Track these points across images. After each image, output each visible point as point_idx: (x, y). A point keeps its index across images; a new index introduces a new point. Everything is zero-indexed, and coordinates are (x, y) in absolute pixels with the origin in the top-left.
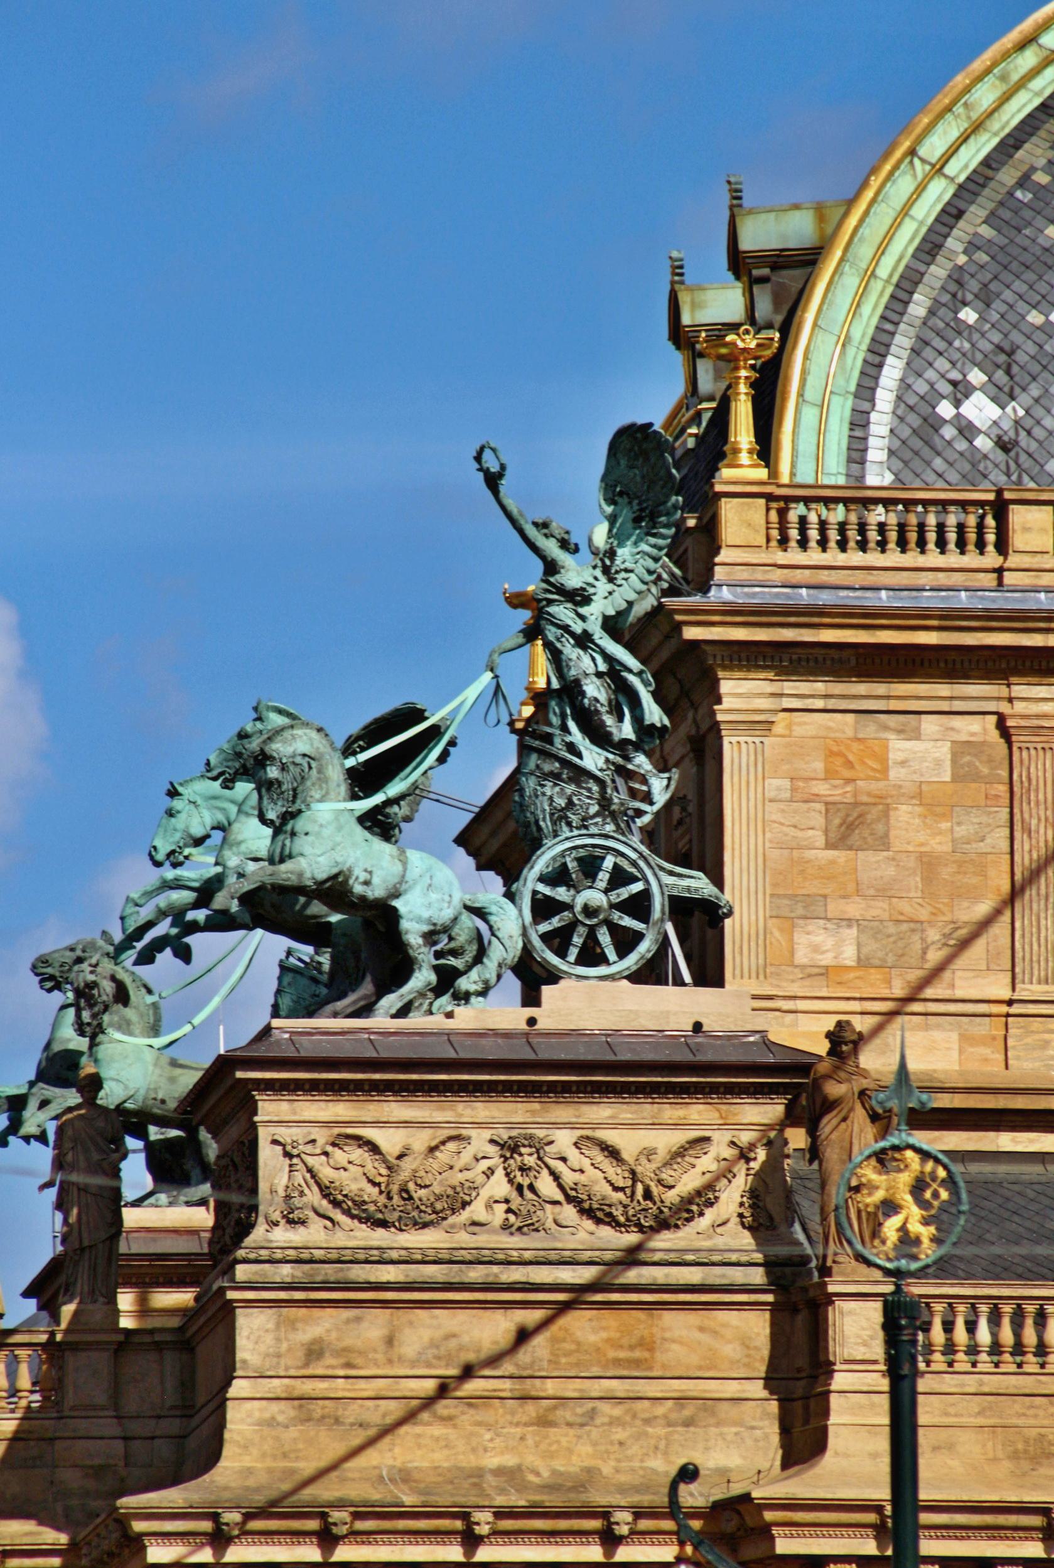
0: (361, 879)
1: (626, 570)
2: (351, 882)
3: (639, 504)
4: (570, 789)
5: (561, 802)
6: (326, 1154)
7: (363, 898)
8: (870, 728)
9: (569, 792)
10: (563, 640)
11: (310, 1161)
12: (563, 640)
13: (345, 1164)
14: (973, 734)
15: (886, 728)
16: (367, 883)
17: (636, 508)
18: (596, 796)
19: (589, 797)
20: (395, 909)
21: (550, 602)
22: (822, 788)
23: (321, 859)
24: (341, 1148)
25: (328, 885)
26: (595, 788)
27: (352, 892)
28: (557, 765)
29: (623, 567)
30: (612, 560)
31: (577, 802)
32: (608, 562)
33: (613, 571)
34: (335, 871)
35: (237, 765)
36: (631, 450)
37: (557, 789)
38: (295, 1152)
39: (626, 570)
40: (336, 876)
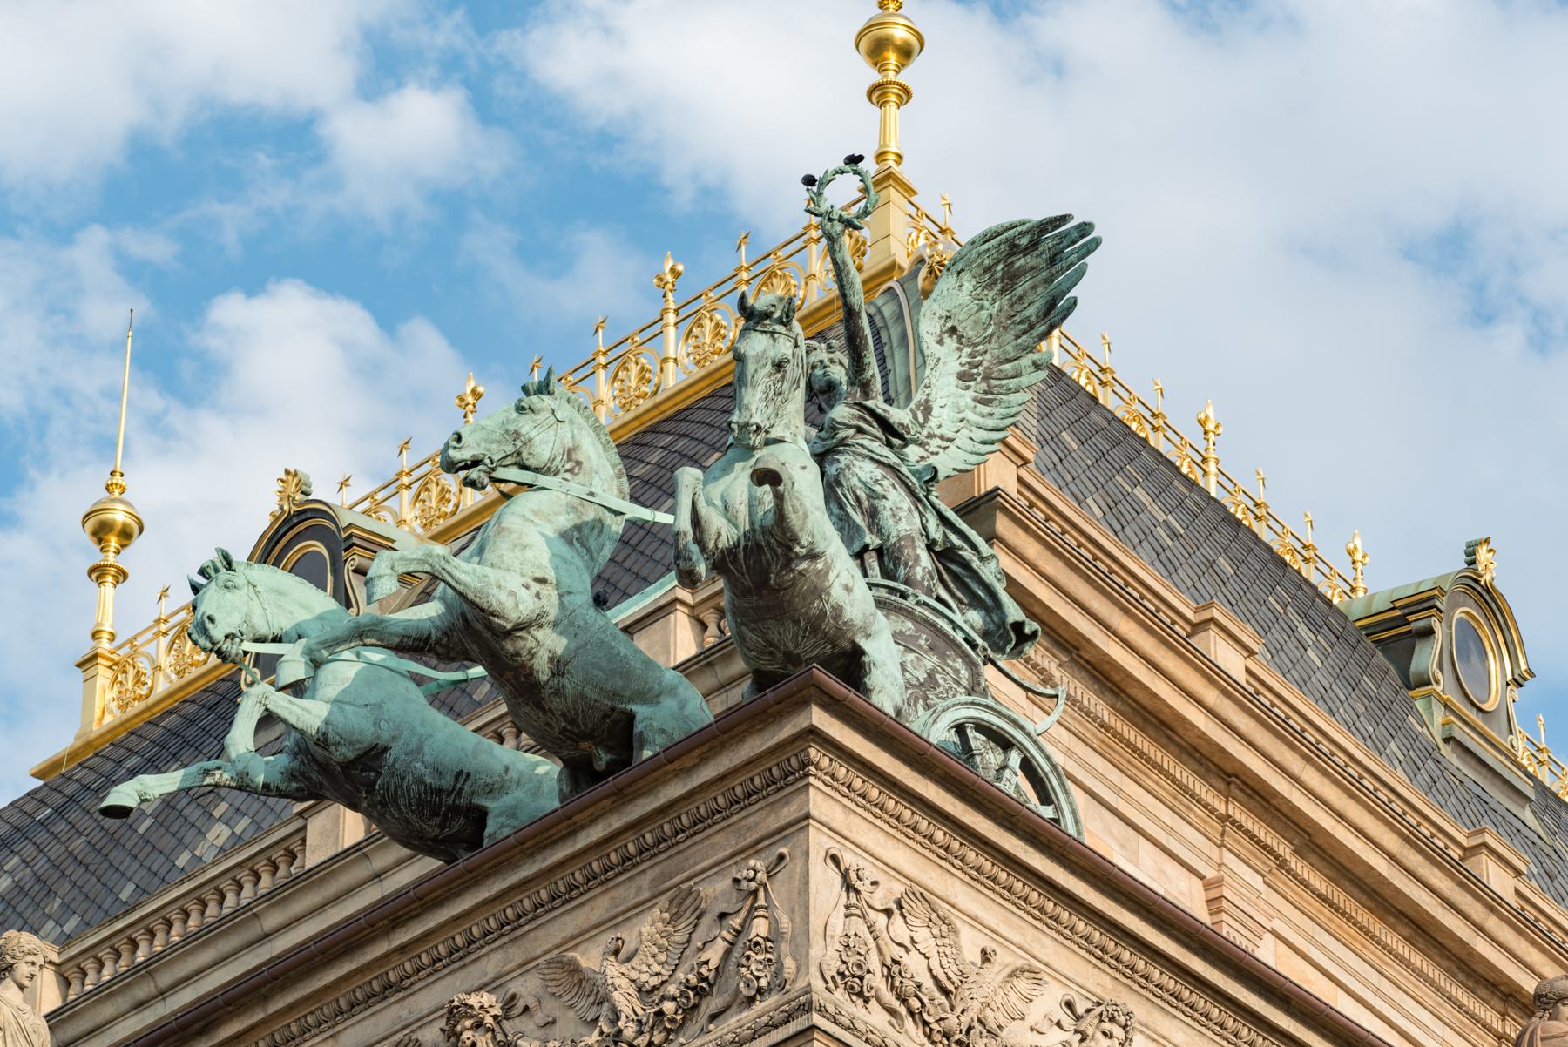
1: (942, 438)
2: (832, 576)
3: (970, 355)
4: (931, 661)
5: (922, 676)
6: (888, 912)
7: (838, 611)
9: (930, 665)
10: (885, 483)
11: (872, 915)
12: (885, 483)
13: (908, 943)
14: (1182, 893)
17: (965, 360)
18: (964, 682)
19: (958, 683)
20: (863, 653)
21: (860, 430)
24: (904, 917)
26: (964, 673)
27: (829, 594)
28: (910, 624)
29: (938, 432)
30: (926, 420)
31: (941, 682)
35: (510, 449)
36: (988, 269)
37: (911, 656)
38: (858, 885)
39: (942, 438)
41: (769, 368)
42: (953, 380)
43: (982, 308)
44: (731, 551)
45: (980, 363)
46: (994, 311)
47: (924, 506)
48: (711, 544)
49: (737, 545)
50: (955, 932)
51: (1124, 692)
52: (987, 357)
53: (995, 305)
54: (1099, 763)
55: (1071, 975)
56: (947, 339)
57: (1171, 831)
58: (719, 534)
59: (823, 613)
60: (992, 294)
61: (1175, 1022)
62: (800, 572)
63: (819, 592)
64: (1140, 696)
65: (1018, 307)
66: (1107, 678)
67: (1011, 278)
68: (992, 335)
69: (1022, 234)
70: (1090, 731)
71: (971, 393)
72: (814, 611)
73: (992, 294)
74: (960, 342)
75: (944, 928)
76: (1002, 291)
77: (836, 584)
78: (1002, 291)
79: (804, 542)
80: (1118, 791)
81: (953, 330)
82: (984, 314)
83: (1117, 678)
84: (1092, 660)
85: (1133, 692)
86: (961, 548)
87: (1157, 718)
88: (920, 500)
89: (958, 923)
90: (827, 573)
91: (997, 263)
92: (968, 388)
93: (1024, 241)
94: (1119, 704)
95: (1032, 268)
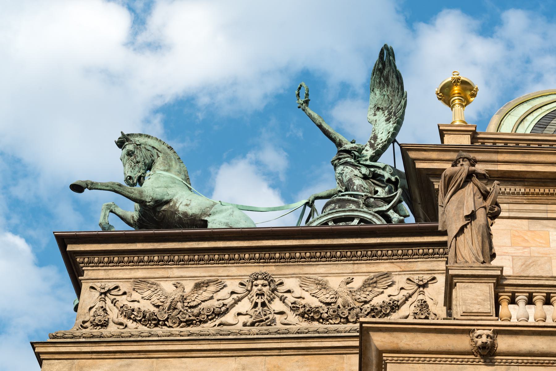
0: (184, 203)
2: (177, 205)
7: (185, 214)
8: (537, 225)
15: (547, 226)
16: (187, 205)
17: (386, 115)
22: (511, 250)
23: (157, 189)
25: (165, 207)
27: (178, 211)
32: (373, 142)
33: (376, 145)
34: (166, 198)
36: (380, 82)
40: (167, 202)
41: (126, 157)
42: (385, 123)
43: (384, 95)
44: (139, 220)
45: (392, 112)
46: (389, 93)
47: (359, 167)
48: (132, 221)
49: (140, 216)
50: (158, 285)
51: (526, 178)
52: (393, 108)
53: (387, 91)
54: (531, 207)
55: (243, 274)
56: (378, 113)
57: (547, 211)
58: (133, 217)
59: (180, 217)
60: (385, 89)
61: (319, 266)
62: (163, 211)
63: (174, 212)
64: (533, 176)
65: (393, 87)
66: (513, 178)
67: (387, 79)
68: (391, 101)
69: (378, 64)
70: (519, 199)
71: (392, 122)
72: (177, 219)
73: (385, 89)
74: (383, 110)
75: (155, 286)
76: (388, 86)
77: (181, 206)
78: (388, 86)
79: (148, 200)
80: (547, 211)
81: (378, 109)
82: (386, 97)
83: (517, 176)
84: (500, 176)
85: (528, 176)
86: (375, 171)
87: (549, 179)
88: (357, 166)
89: (158, 282)
90: (175, 204)
91: (380, 79)
92: (390, 122)
93: (380, 66)
94: (526, 184)
95: (389, 72)
